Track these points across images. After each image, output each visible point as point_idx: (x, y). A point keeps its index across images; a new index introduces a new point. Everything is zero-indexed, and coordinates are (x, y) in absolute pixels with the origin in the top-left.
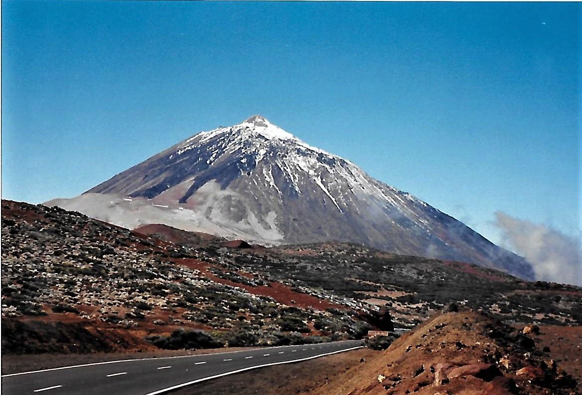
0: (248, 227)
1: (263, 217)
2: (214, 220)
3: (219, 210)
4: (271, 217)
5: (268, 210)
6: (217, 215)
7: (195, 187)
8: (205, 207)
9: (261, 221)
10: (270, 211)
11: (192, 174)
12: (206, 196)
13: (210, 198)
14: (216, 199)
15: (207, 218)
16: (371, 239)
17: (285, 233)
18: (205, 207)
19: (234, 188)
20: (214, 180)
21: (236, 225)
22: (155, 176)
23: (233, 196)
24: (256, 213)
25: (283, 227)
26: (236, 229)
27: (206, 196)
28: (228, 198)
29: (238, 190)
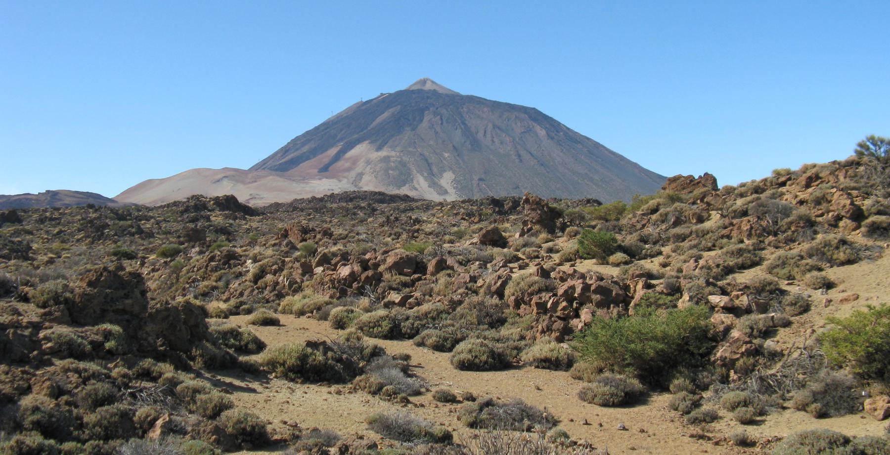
5: (442, 171)
7: (343, 151)
8: (353, 174)
9: (434, 185)
10: (445, 171)
11: (341, 139)
12: (355, 161)
14: (368, 162)
18: (353, 174)
19: (393, 148)
22: (297, 150)
24: (426, 174)
27: (355, 161)
28: (386, 159)
29: (398, 149)
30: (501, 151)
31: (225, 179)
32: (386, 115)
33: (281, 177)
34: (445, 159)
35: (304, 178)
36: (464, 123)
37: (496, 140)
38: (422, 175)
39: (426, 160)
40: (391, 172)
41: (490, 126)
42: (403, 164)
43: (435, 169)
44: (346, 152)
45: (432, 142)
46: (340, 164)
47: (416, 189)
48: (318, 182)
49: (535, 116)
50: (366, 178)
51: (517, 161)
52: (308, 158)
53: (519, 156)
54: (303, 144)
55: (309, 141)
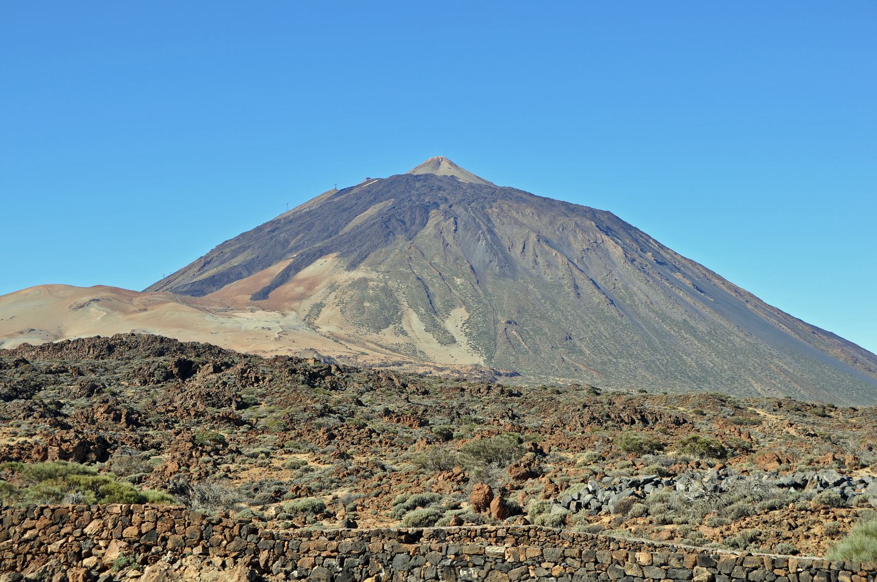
0: (401, 340)
3: (338, 308)
4: (456, 321)
5: (450, 306)
6: (330, 320)
8: (306, 305)
9: (434, 327)
10: (453, 307)
11: (296, 249)
12: (312, 285)
14: (333, 287)
18: (306, 305)
19: (374, 266)
20: (335, 254)
21: (374, 336)
22: (224, 262)
23: (372, 280)
24: (422, 310)
25: (482, 337)
27: (312, 285)
29: (383, 268)
30: (548, 278)
31: (95, 304)
32: (372, 211)
33: (189, 304)
34: (456, 287)
35: (228, 308)
36: (491, 231)
37: (540, 260)
38: (417, 311)
39: (426, 288)
40: (367, 304)
41: (533, 237)
42: (387, 292)
43: (438, 303)
44: (298, 270)
45: (437, 260)
46: (290, 288)
47: (404, 333)
48: (249, 315)
49: (610, 225)
50: (326, 312)
51: (572, 295)
52: (239, 276)
53: (576, 287)
54: (235, 253)
55: (244, 249)
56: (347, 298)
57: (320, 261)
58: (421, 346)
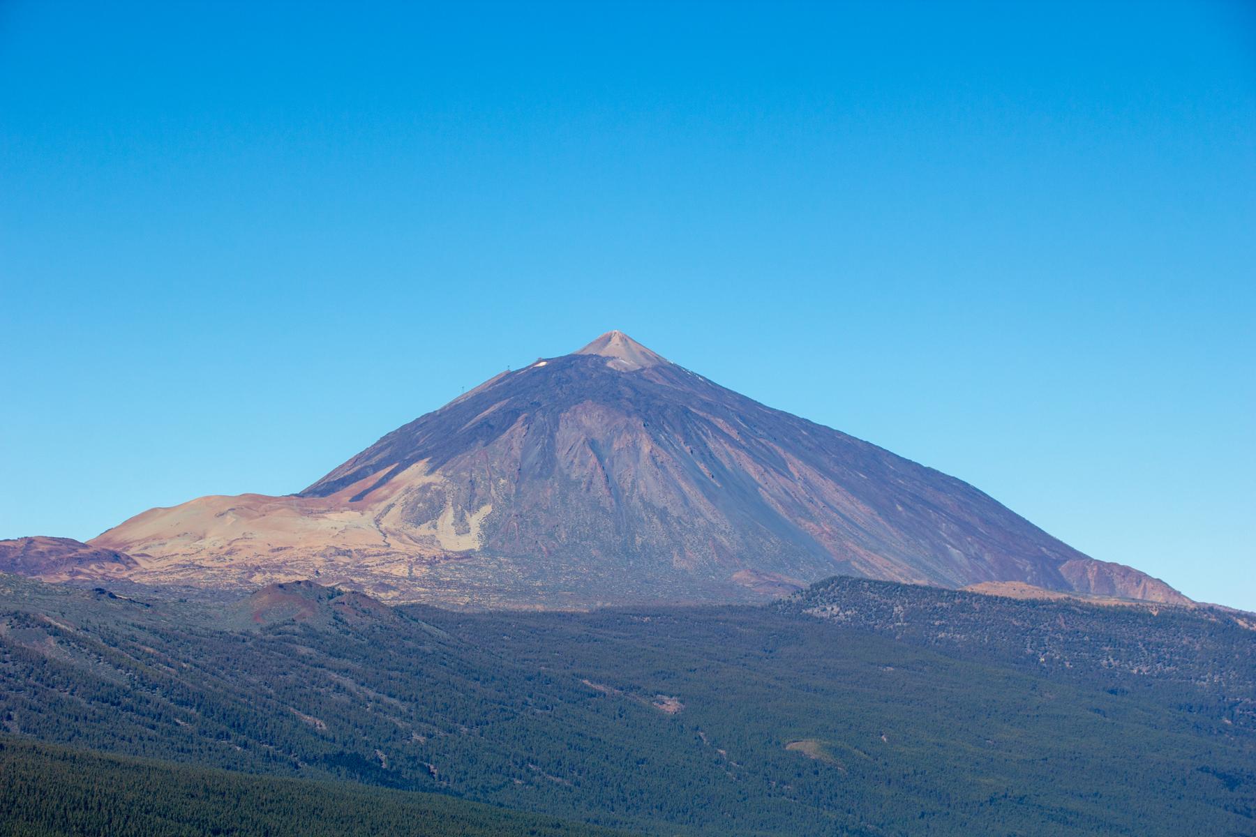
0: (433, 531)
1: (467, 514)
2: (382, 526)
5: (483, 502)
7: (394, 473)
13: (400, 491)
15: (377, 521)
16: (639, 540)
17: (488, 537)
25: (490, 528)
26: (405, 537)
28: (425, 488)
30: (573, 477)
43: (476, 502)
46: (383, 491)
47: (435, 527)
56: (411, 499)
57: (414, 466)
58: (438, 537)
